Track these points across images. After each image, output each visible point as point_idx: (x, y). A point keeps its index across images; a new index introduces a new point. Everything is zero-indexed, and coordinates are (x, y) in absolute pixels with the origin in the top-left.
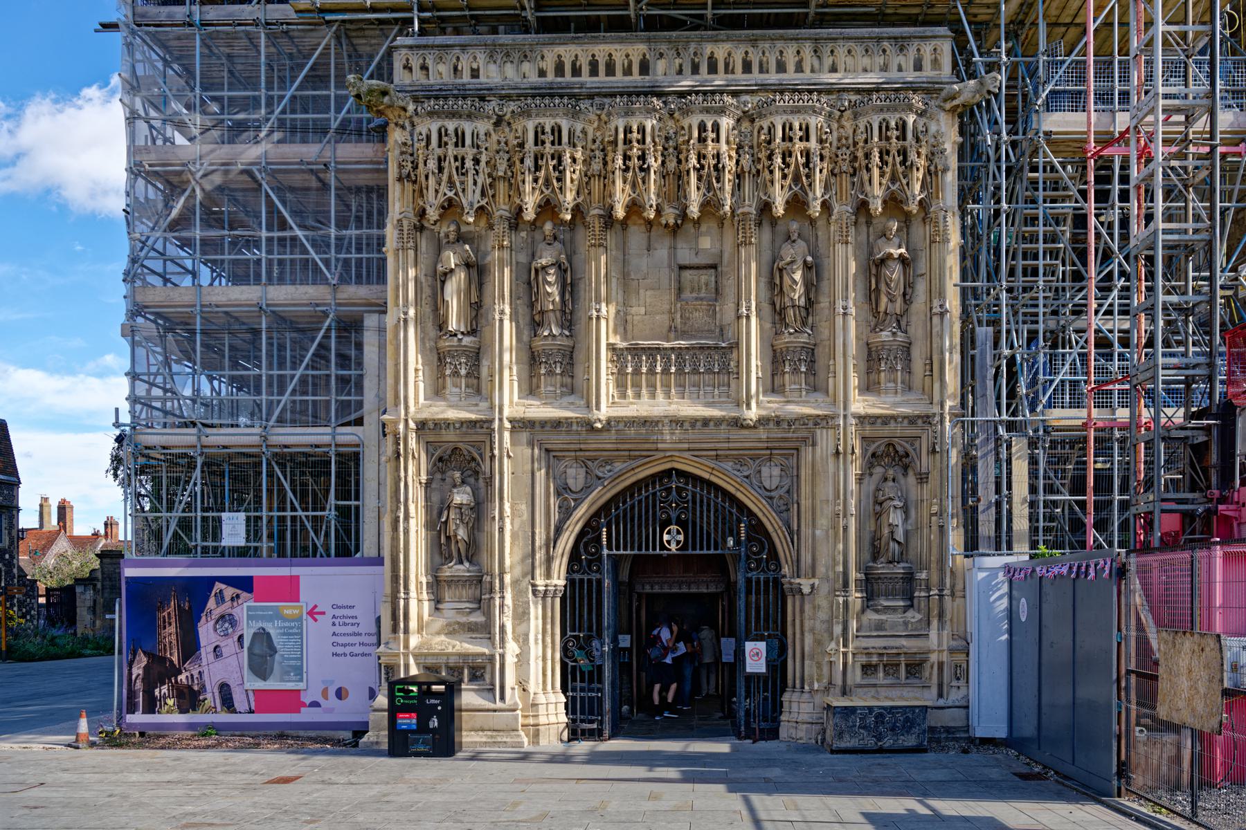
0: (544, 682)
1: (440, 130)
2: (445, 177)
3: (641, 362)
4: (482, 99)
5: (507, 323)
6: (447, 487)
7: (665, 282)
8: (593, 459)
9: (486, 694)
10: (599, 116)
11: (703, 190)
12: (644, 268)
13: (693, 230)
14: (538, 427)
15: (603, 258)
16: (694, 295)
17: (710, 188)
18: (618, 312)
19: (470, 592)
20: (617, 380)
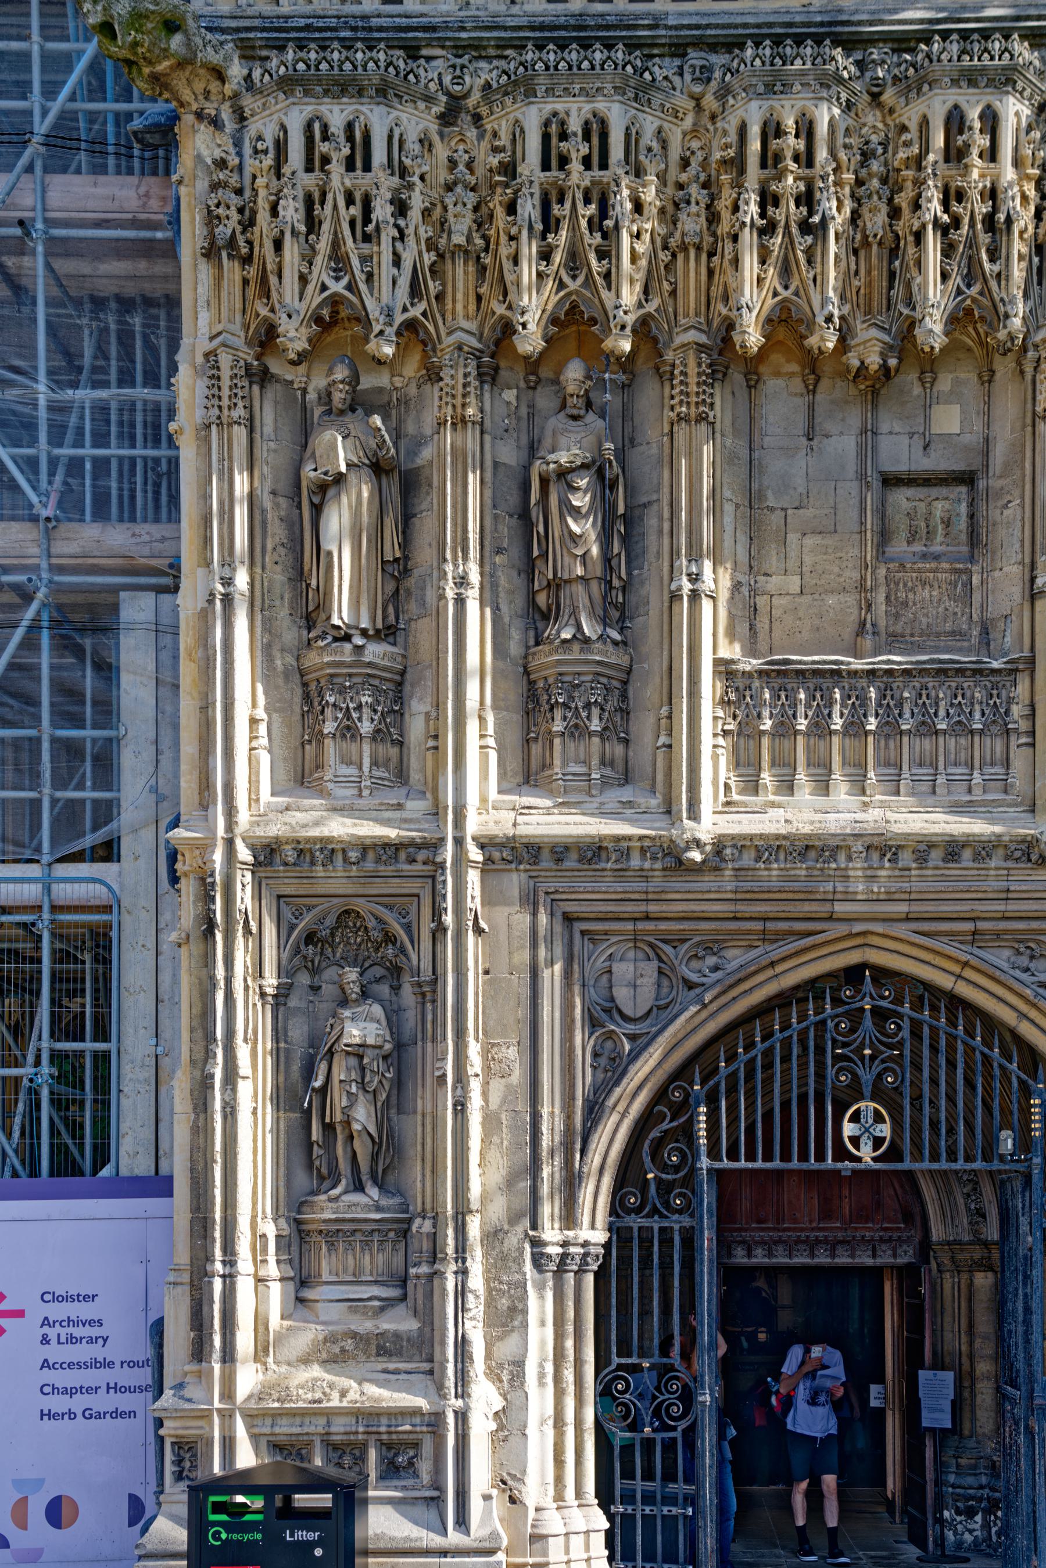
0: (559, 1480)
1: (309, 127)
2: (323, 245)
3: (794, 706)
4: (412, 52)
5: (473, 607)
6: (324, 1007)
7: (849, 515)
8: (676, 941)
9: (420, 1510)
10: (697, 99)
11: (956, 280)
12: (800, 482)
13: (917, 390)
14: (546, 862)
15: (707, 451)
16: (918, 547)
17: (972, 274)
18: (736, 586)
19: (380, 1258)
20: (735, 751)
